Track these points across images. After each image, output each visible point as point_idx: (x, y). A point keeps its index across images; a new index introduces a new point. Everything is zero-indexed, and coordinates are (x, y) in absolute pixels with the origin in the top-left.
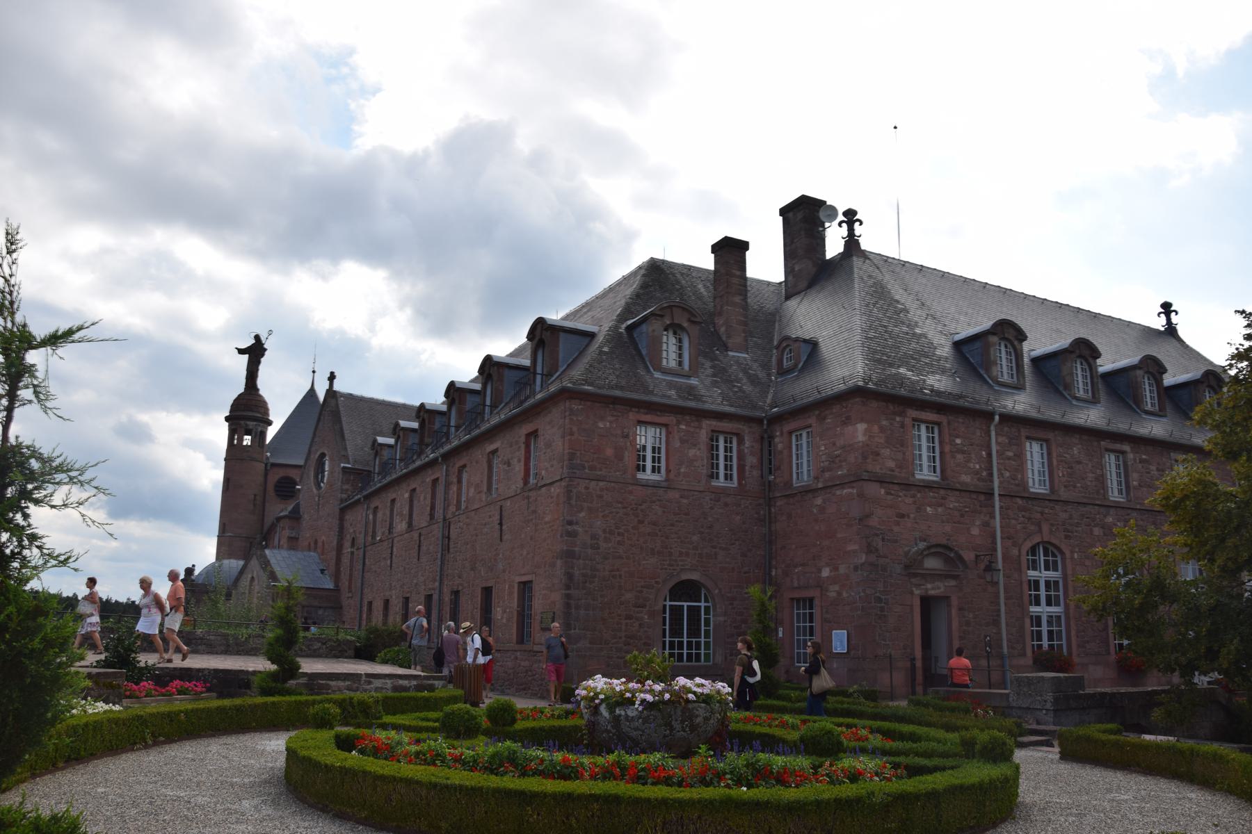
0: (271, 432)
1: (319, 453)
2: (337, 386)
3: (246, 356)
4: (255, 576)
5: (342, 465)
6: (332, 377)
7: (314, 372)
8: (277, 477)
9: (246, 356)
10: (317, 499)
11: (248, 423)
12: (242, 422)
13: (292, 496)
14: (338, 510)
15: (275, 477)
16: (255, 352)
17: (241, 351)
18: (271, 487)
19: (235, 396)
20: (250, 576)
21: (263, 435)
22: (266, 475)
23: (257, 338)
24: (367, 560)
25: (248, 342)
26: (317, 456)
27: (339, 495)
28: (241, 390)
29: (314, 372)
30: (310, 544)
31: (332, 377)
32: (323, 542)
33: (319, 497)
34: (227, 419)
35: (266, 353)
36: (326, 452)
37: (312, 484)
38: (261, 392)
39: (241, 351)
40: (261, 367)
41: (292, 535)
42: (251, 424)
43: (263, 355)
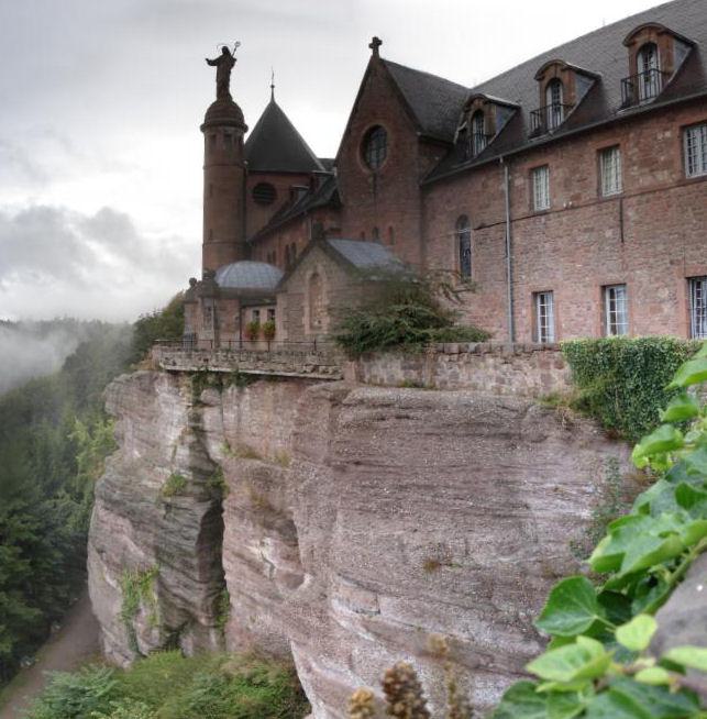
0: (246, 137)
1: (367, 128)
2: (384, 53)
3: (215, 68)
4: (320, 269)
5: (419, 133)
6: (376, 43)
7: (273, 87)
8: (255, 183)
9: (215, 68)
10: (371, 180)
11: (227, 128)
12: (220, 128)
13: (269, 203)
14: (417, 188)
15: (253, 182)
16: (224, 63)
17: (211, 63)
18: (249, 192)
19: (208, 106)
20: (309, 273)
21: (241, 138)
22: (245, 183)
23: (225, 50)
24: (517, 239)
25: (217, 54)
26: (364, 132)
27: (417, 170)
28: (214, 98)
29: (273, 87)
30: (363, 234)
31: (376, 43)
32: (391, 229)
33: (375, 176)
34: (203, 128)
35: (236, 63)
36: (381, 123)
37: (361, 167)
38: (234, 100)
39: (211, 63)
40: (232, 77)
41: (335, 226)
42: (231, 130)
43: (233, 65)
